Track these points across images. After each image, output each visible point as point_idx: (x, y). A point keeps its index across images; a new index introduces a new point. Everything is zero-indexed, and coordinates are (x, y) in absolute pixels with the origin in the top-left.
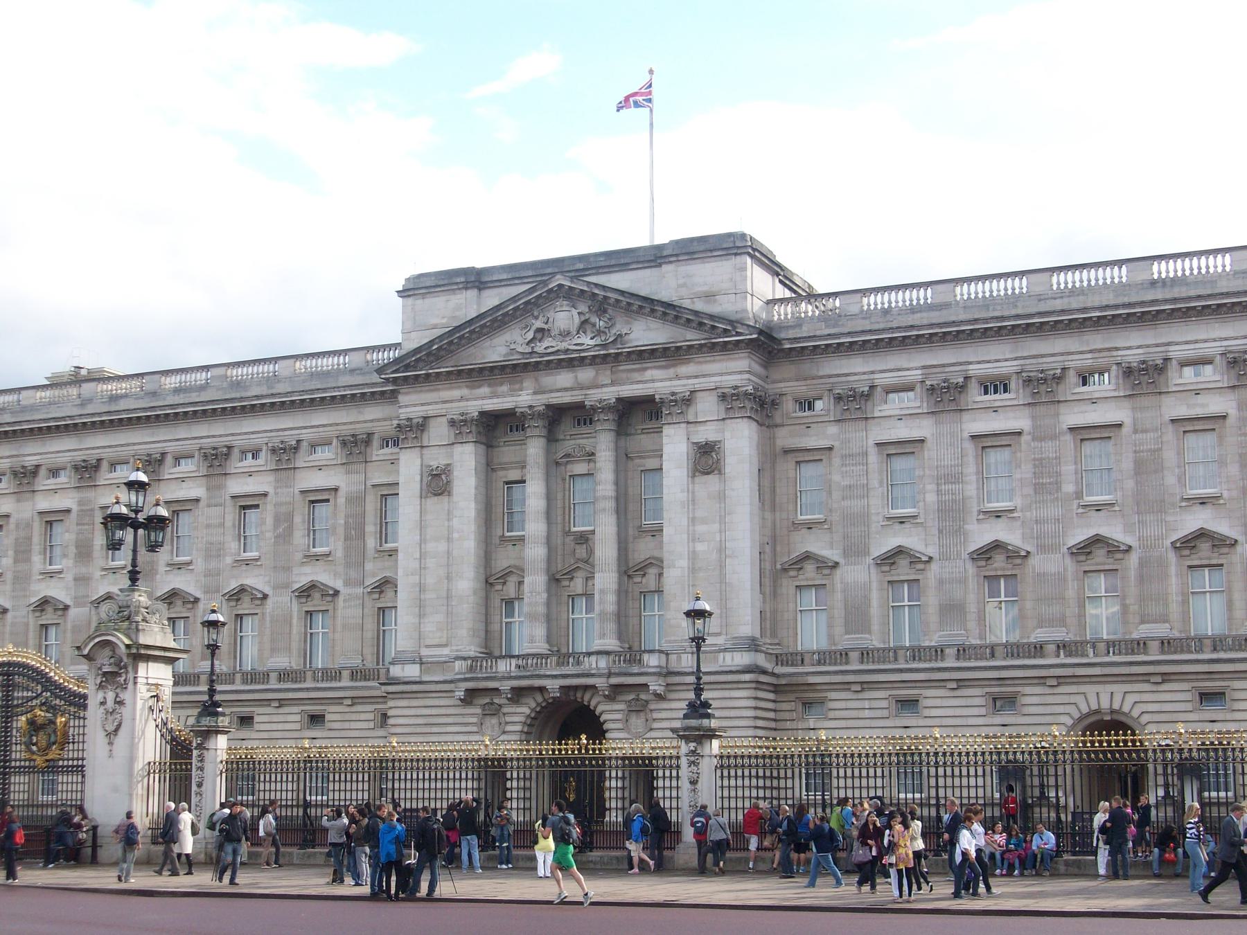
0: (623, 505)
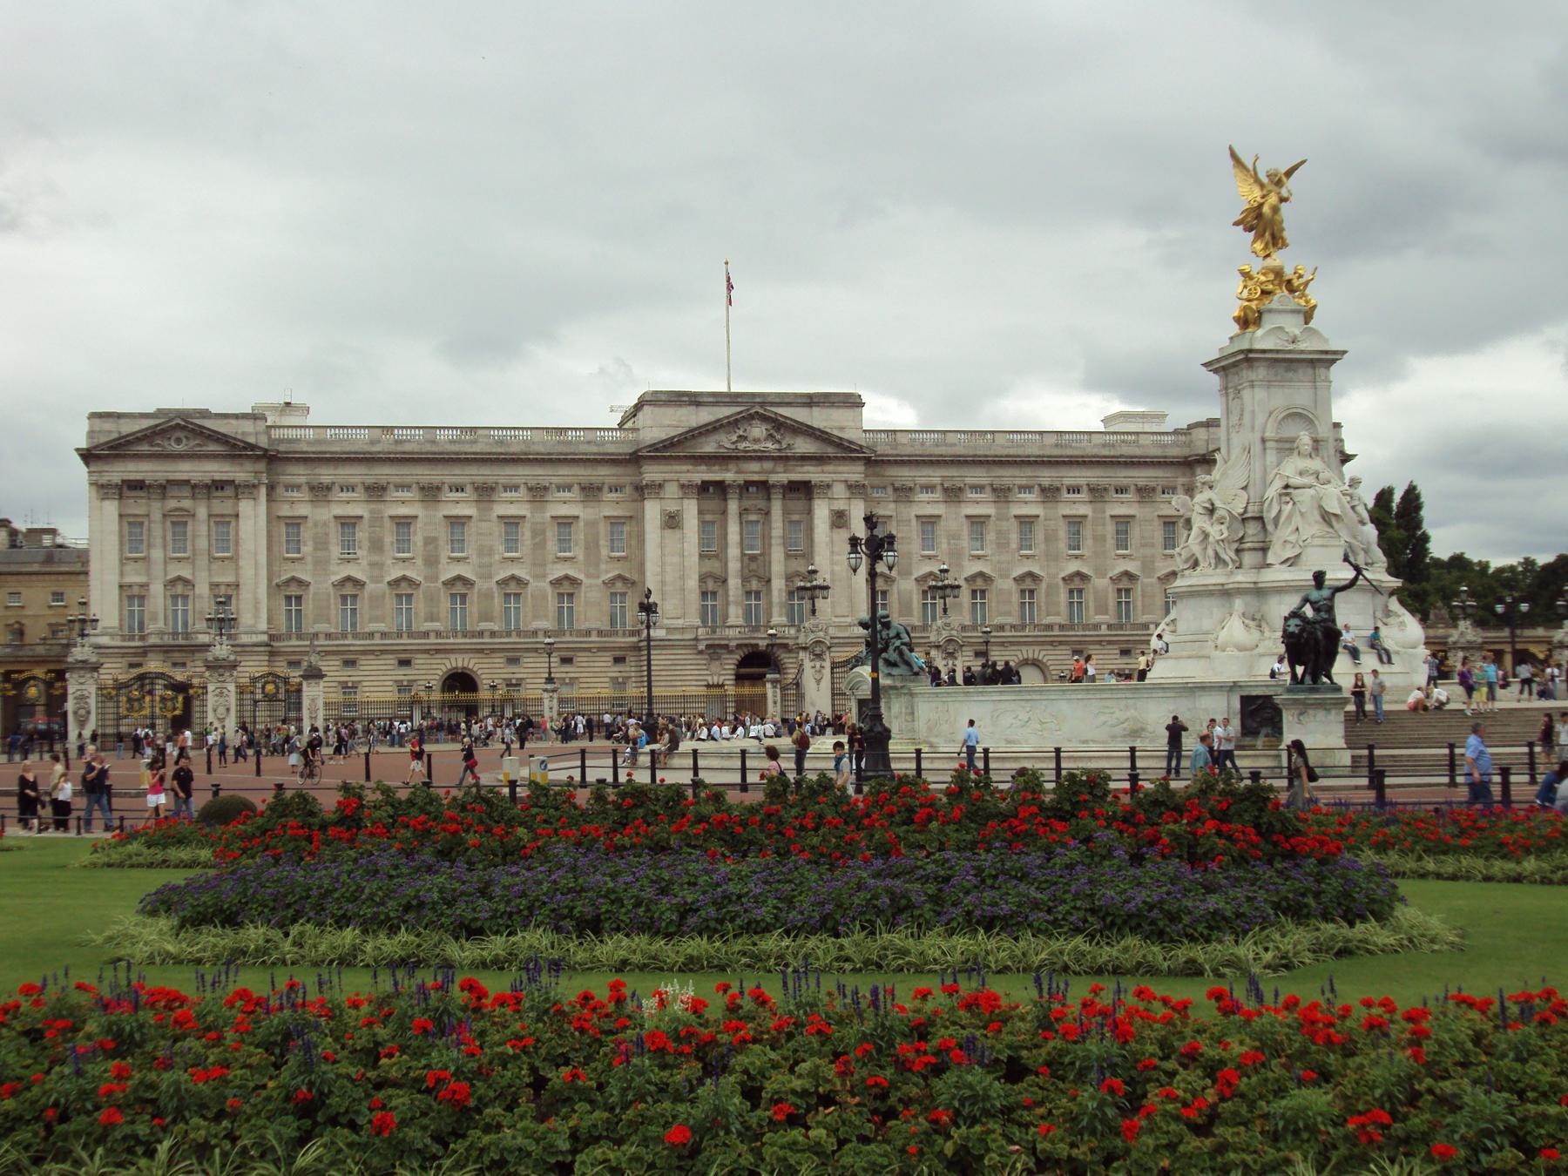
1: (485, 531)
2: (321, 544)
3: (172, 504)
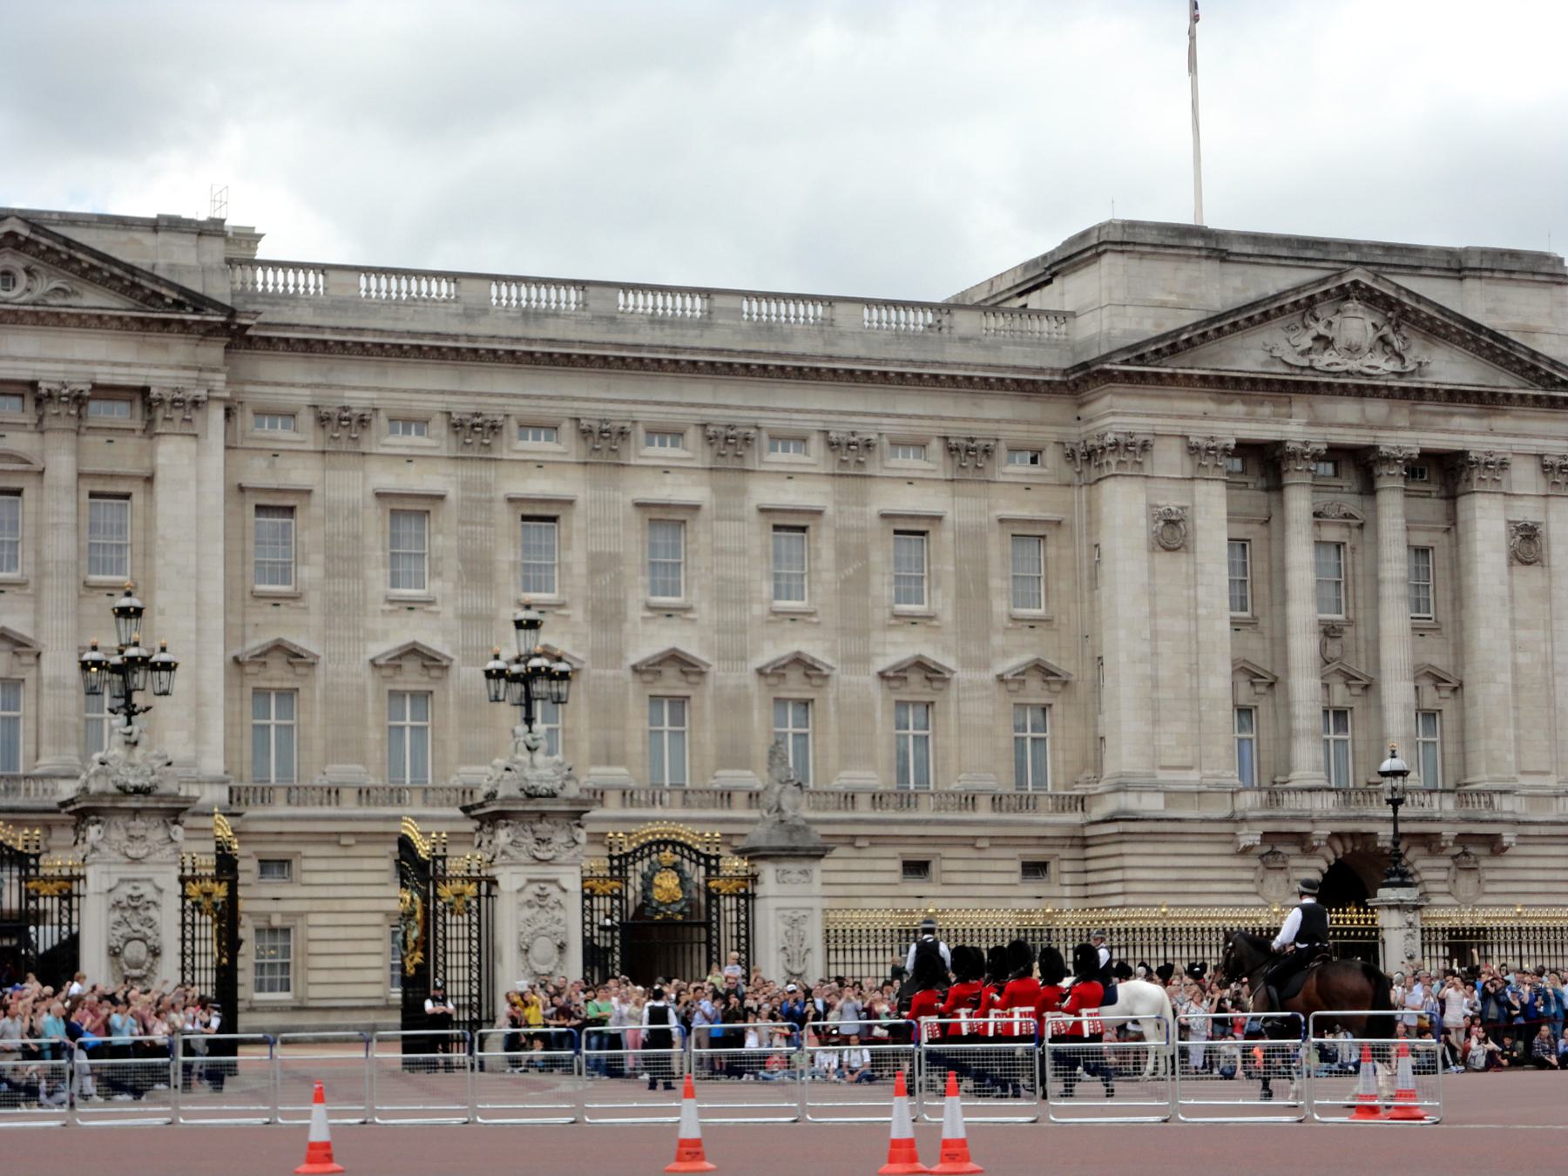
1: (731, 545)
2: (345, 562)
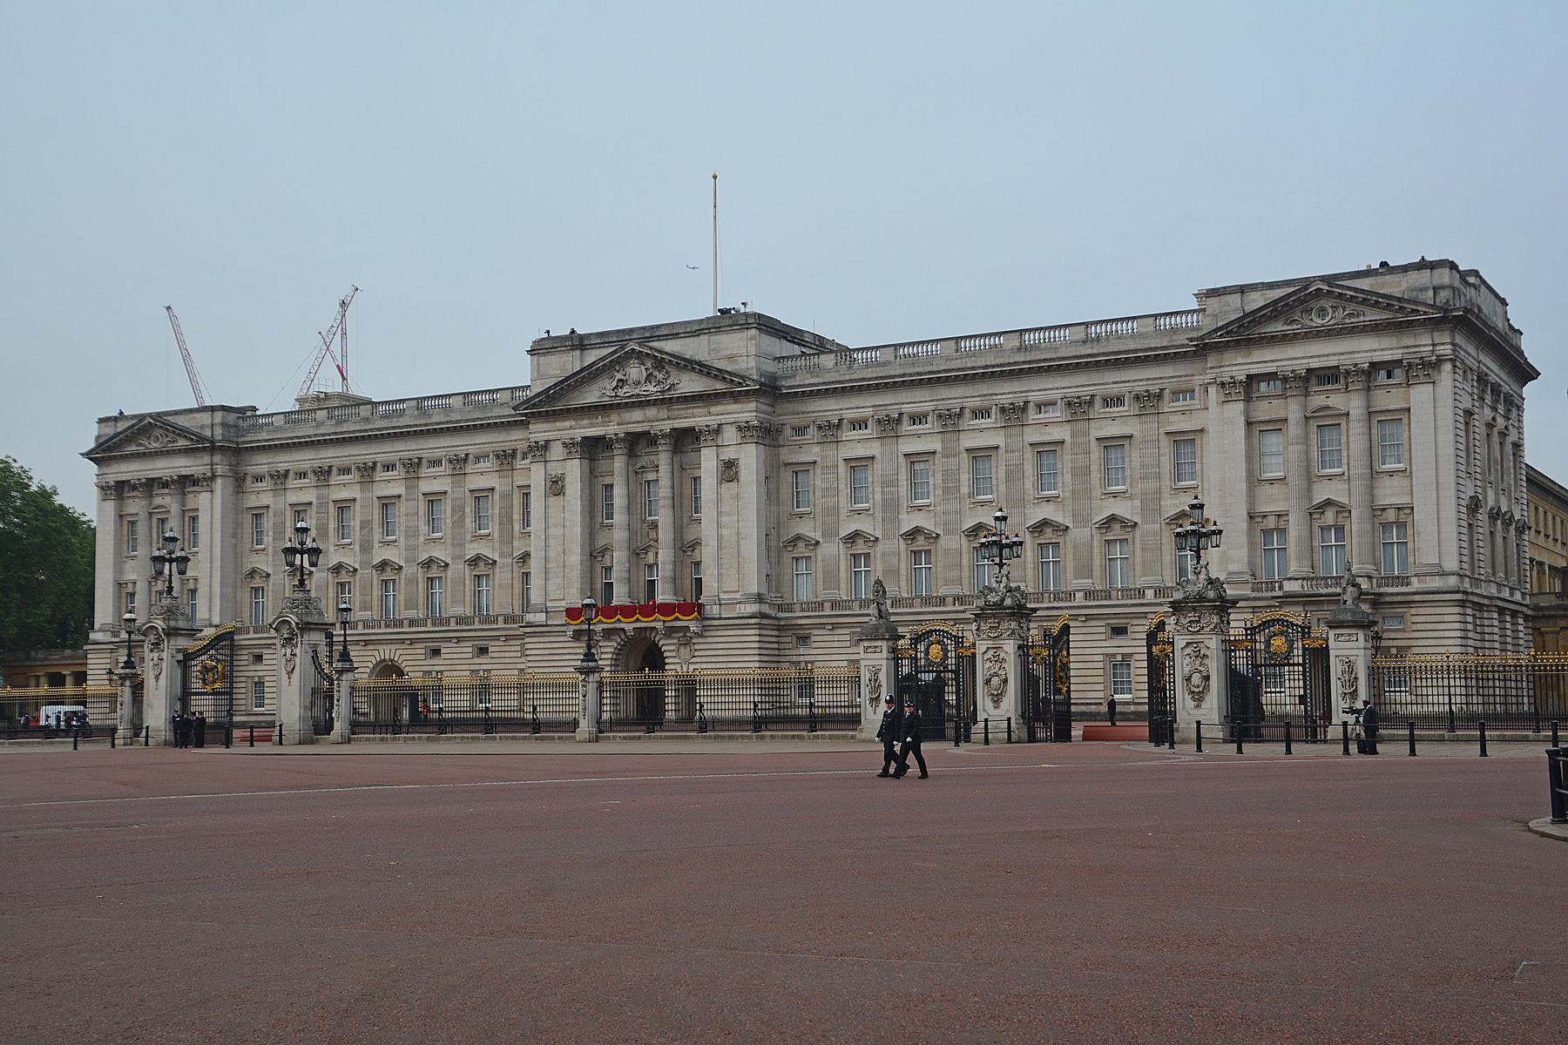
0: (676, 502)
1: (410, 513)
3: (158, 501)
